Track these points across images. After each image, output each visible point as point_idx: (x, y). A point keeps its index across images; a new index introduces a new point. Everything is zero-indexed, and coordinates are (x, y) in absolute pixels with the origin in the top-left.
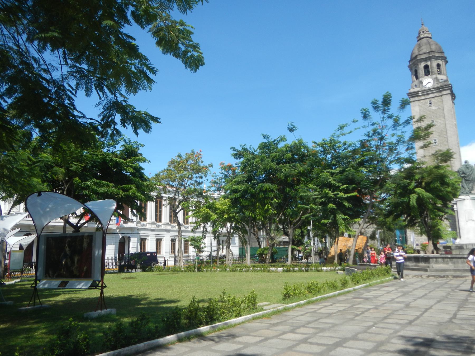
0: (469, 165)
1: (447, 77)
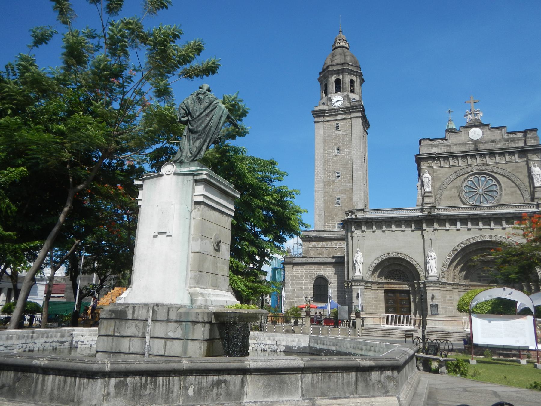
1: (361, 97)
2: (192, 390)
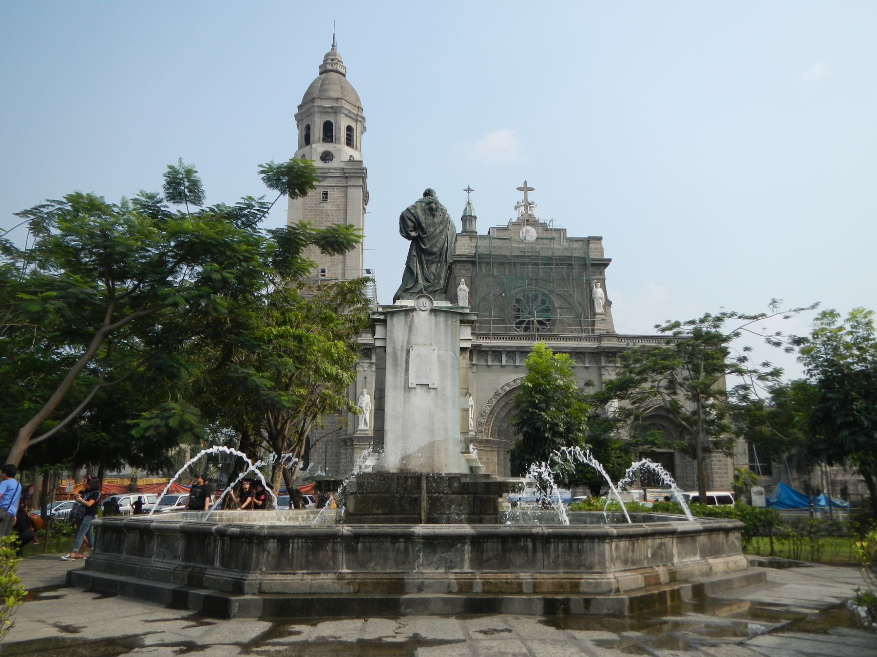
0: (437, 203)
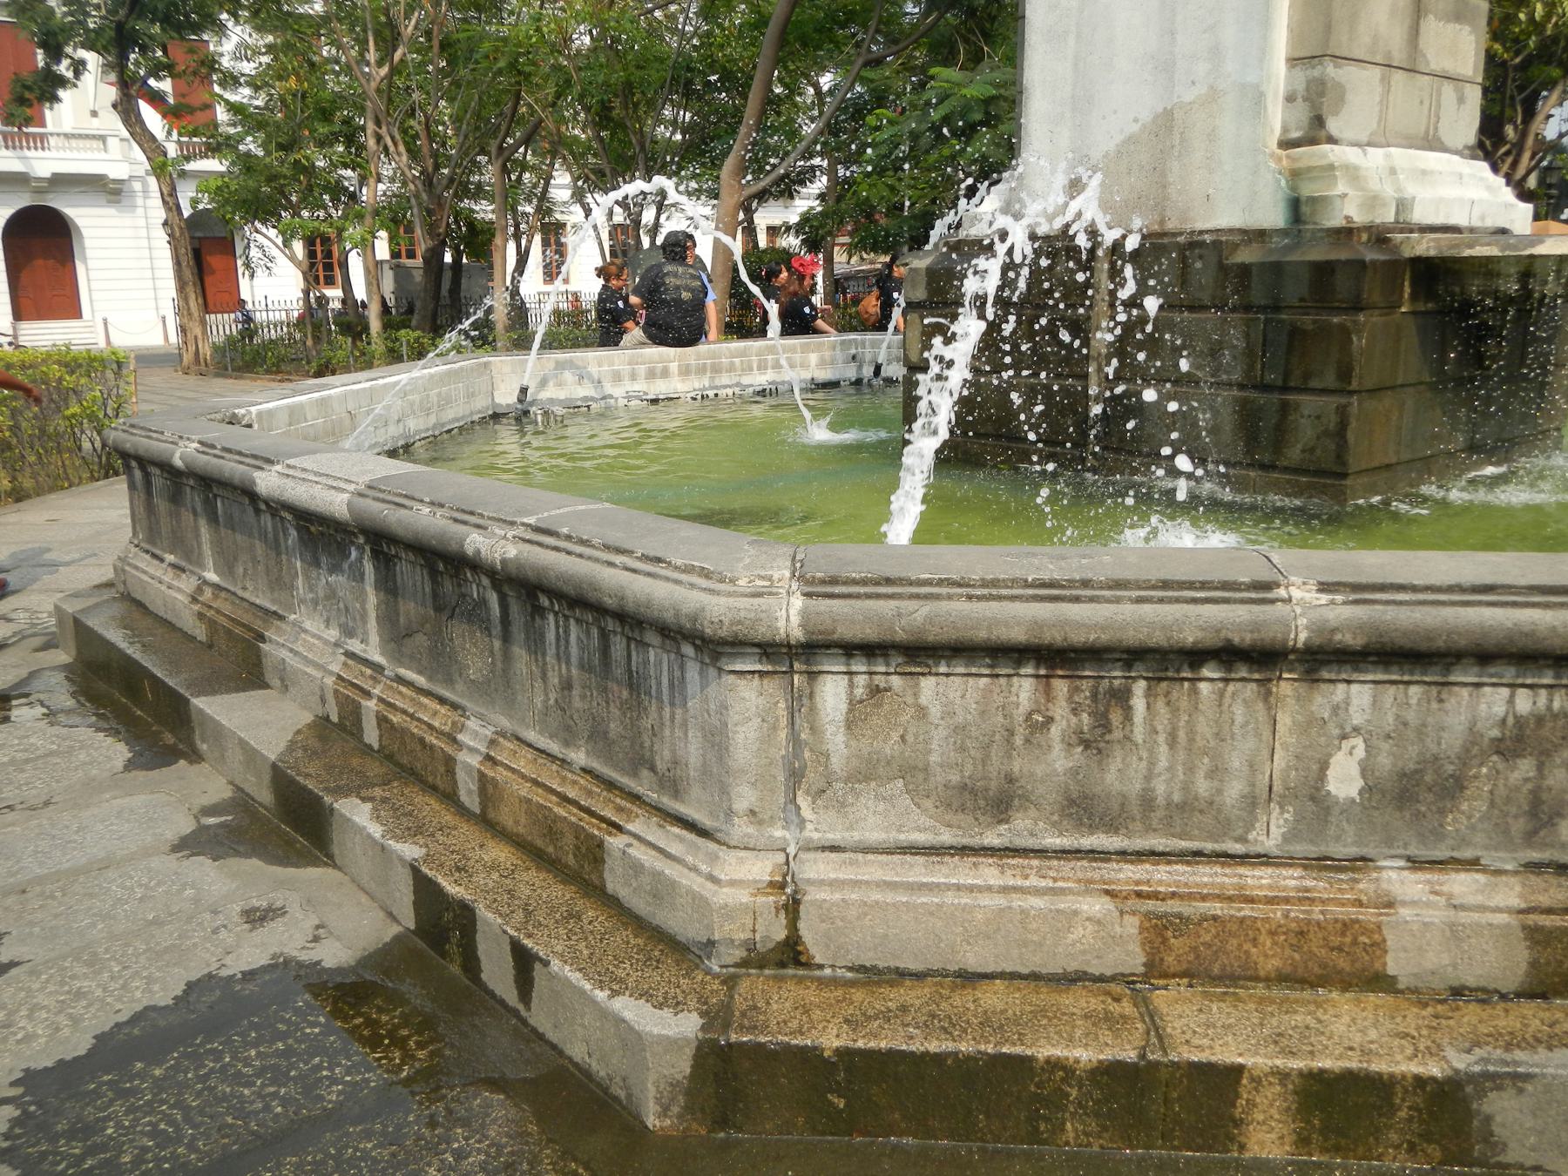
2: (1355, 771)
